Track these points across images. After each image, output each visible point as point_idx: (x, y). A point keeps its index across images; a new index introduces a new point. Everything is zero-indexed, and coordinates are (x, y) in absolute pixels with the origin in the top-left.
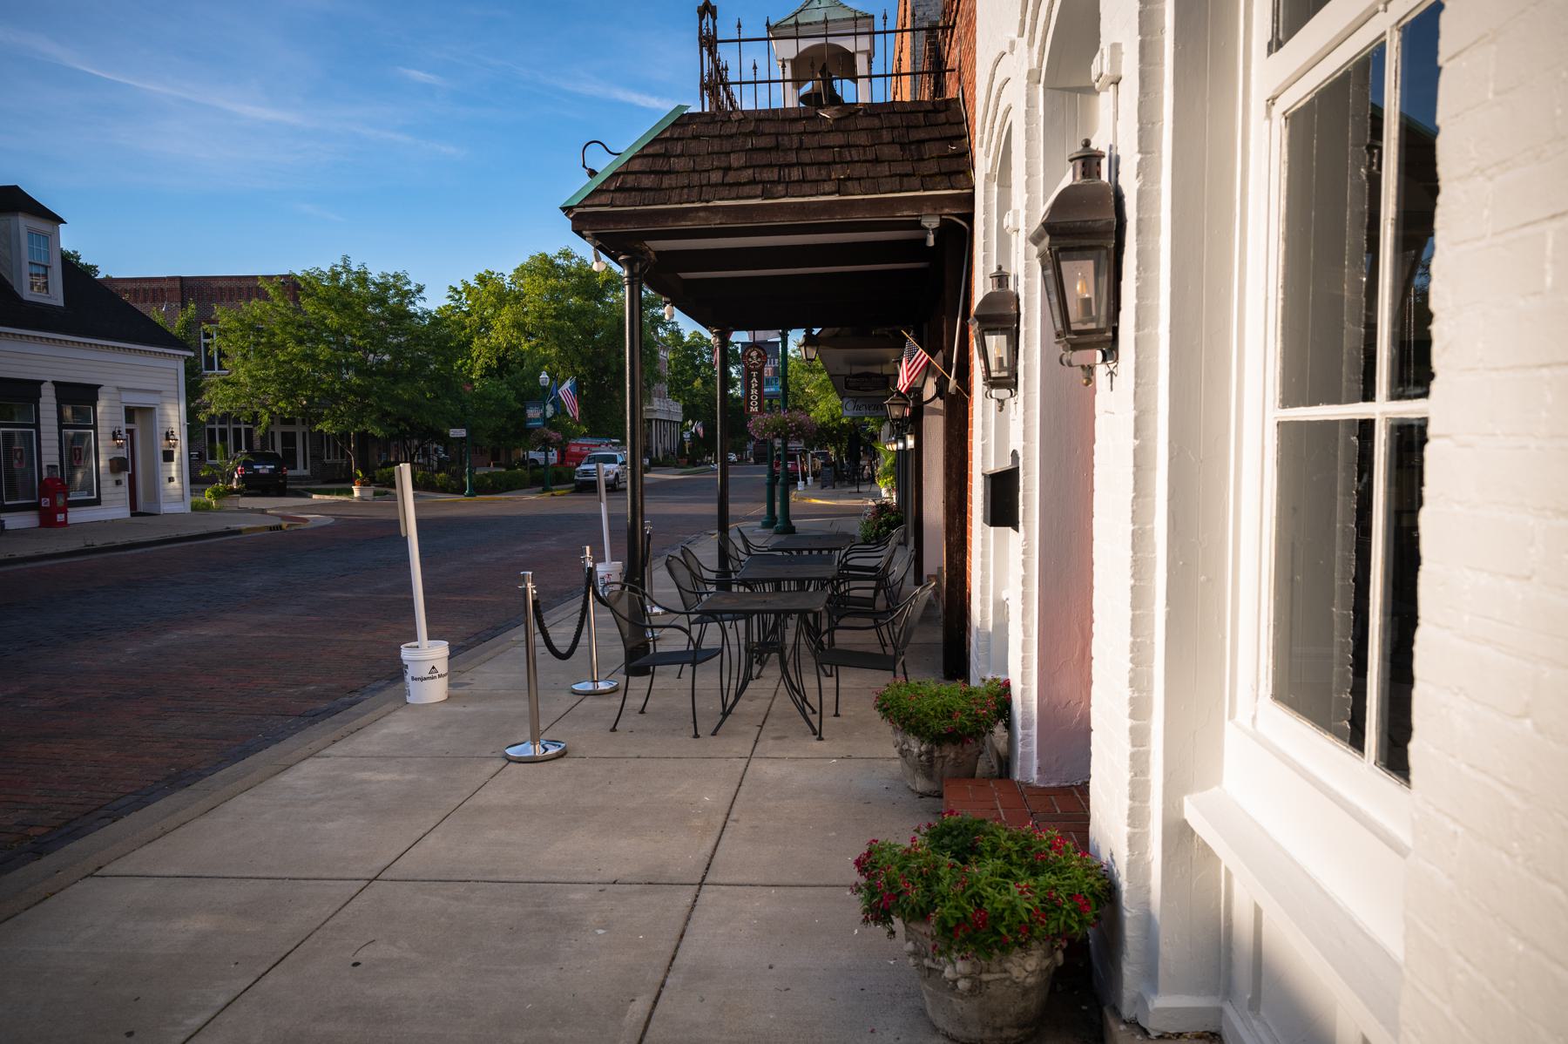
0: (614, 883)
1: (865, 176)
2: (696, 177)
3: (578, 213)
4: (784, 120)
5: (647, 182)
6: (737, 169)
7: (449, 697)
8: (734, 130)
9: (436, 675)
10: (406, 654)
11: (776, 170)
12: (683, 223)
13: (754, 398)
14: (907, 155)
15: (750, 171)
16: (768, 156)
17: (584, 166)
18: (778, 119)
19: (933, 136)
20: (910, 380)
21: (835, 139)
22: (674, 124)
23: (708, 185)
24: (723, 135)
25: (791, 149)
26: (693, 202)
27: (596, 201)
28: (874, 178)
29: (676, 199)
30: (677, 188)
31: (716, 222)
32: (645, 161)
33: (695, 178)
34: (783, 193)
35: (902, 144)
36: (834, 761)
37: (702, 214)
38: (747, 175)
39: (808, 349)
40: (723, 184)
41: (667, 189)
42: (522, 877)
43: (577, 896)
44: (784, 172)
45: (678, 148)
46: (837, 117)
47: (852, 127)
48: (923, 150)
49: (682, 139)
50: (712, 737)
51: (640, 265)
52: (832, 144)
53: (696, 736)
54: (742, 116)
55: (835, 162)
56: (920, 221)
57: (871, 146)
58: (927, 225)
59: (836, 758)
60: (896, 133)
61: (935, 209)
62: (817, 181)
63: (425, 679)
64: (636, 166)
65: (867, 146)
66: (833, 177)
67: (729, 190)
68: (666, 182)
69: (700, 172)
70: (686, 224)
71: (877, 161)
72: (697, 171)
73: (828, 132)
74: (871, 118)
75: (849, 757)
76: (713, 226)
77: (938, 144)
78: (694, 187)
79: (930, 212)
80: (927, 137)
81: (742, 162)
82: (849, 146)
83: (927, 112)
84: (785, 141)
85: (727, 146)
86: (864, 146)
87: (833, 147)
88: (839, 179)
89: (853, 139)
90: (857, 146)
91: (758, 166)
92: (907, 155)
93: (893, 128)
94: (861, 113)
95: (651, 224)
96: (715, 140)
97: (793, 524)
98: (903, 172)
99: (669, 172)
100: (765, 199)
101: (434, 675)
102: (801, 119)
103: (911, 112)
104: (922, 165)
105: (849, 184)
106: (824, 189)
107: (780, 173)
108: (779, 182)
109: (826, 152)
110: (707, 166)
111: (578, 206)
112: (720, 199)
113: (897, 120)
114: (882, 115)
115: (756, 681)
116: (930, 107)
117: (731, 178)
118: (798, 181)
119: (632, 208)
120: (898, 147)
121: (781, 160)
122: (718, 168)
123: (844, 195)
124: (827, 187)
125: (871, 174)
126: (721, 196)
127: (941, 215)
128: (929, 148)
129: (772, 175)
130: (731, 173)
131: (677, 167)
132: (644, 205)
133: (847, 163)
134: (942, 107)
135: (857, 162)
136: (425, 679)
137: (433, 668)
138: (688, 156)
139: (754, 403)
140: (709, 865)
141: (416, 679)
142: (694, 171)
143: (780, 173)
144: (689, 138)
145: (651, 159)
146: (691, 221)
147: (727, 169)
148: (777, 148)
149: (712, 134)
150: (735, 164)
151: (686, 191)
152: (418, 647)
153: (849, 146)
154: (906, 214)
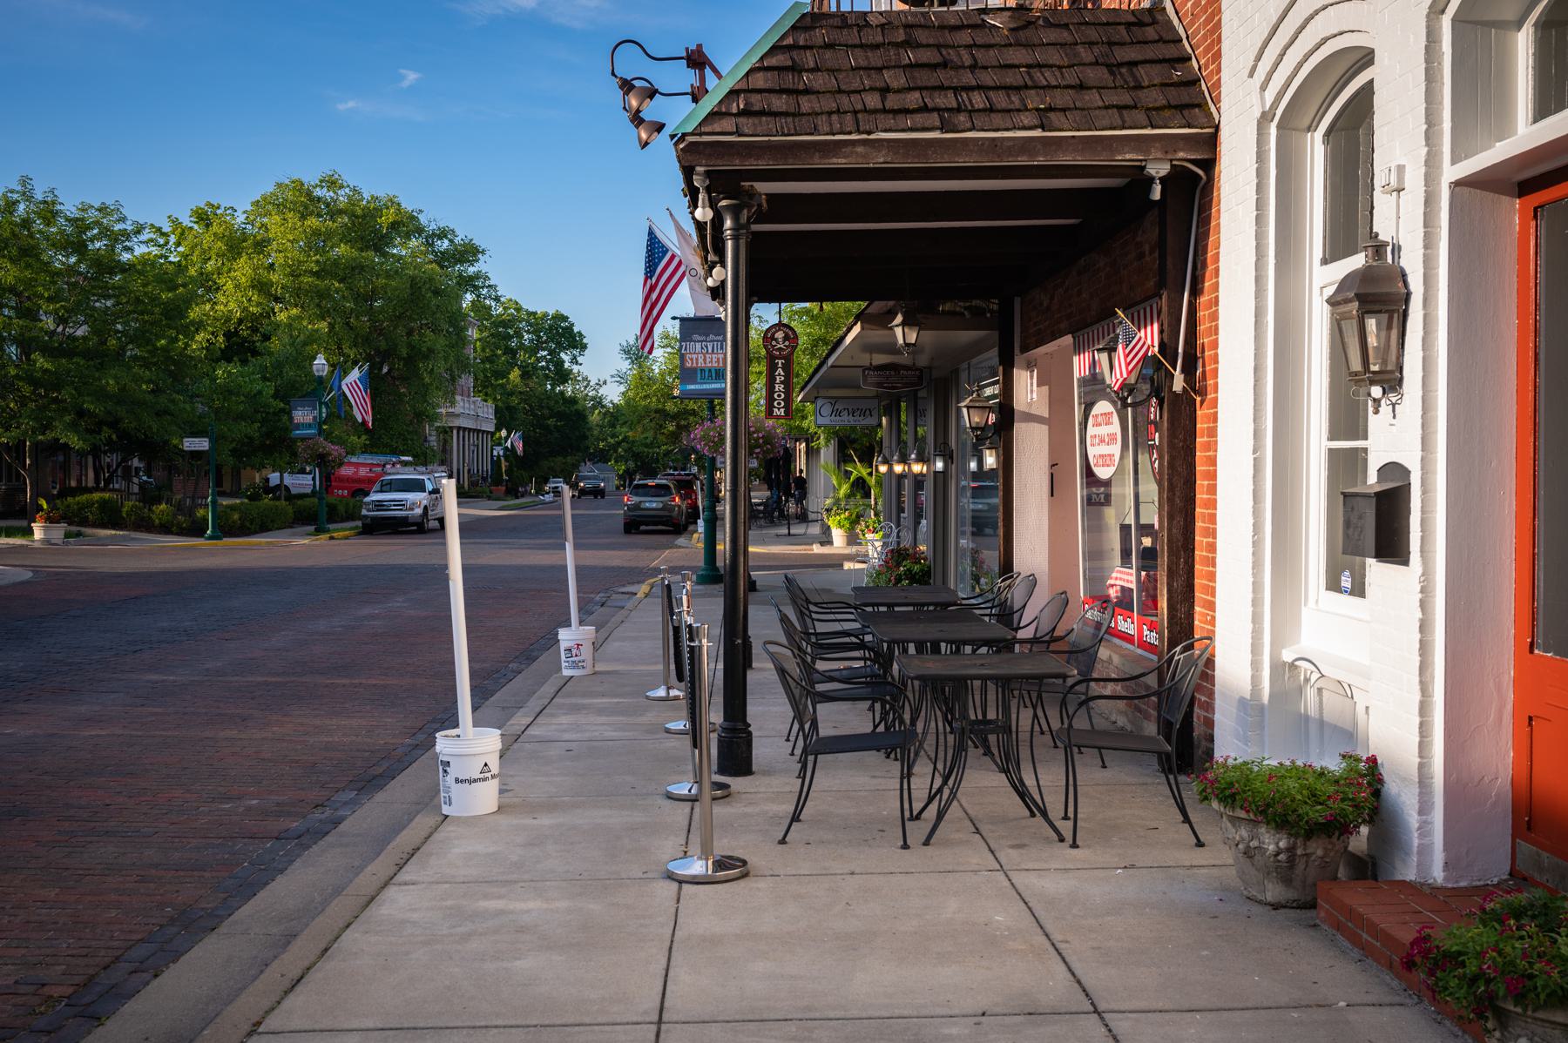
0: (983, 1014)
4: (942, 27)
5: (779, 103)
6: (899, 91)
8: (879, 39)
9: (489, 775)
11: (950, 94)
12: (835, 160)
13: (779, 396)
15: (917, 95)
16: (935, 75)
17: (613, 74)
21: (1017, 56)
22: (794, 28)
23: (865, 111)
24: (867, 46)
25: (963, 67)
26: (850, 133)
29: (827, 129)
30: (822, 113)
31: (879, 160)
32: (769, 74)
33: (845, 102)
34: (969, 125)
36: (1119, 871)
37: (860, 149)
38: (913, 99)
39: (906, 330)
40: (885, 111)
41: (809, 114)
43: (954, 1031)
45: (809, 59)
46: (1012, 26)
47: (1036, 41)
48: (1138, 75)
49: (811, 48)
53: (905, 846)
54: (884, 21)
55: (1026, 87)
56: (1145, 167)
57: (1069, 67)
58: (1153, 172)
60: (1096, 50)
61: (1166, 152)
62: (1009, 111)
63: (475, 781)
64: (760, 81)
65: (1064, 67)
66: (1030, 106)
67: (894, 119)
68: (806, 104)
69: (849, 93)
71: (1081, 87)
72: (844, 92)
73: (1005, 46)
74: (1058, 30)
75: (1133, 866)
76: (871, 165)
77: (1157, 68)
78: (846, 112)
79: (1159, 155)
80: (1140, 58)
81: (902, 81)
82: (1040, 66)
83: (1129, 25)
84: (952, 54)
85: (876, 58)
86: (1060, 67)
87: (1018, 67)
88: (1038, 110)
90: (1051, 66)
91: (926, 88)
93: (1091, 44)
95: (791, 161)
97: (754, 578)
99: (807, 91)
100: (947, 132)
103: (1108, 24)
104: (1141, 94)
105: (1052, 115)
107: (957, 99)
108: (959, 110)
109: (1010, 72)
110: (856, 85)
111: (692, 134)
112: (886, 131)
113: (1093, 34)
114: (1071, 27)
116: (1132, 19)
117: (893, 101)
118: (984, 110)
120: (1105, 70)
121: (955, 80)
122: (872, 89)
123: (1050, 131)
124: (1026, 119)
125: (1078, 104)
126: (888, 127)
127: (1171, 160)
129: (949, 100)
132: (784, 135)
133: (1043, 88)
134: (1147, 19)
135: (1056, 87)
136: (475, 781)
137: (486, 765)
138: (827, 70)
139: (779, 404)
141: (462, 781)
142: (840, 91)
143: (957, 99)
144: (821, 47)
146: (844, 157)
147: (885, 91)
148: (945, 65)
149: (850, 42)
150: (895, 85)
151: (835, 117)
152: (459, 736)
154: (1129, 157)
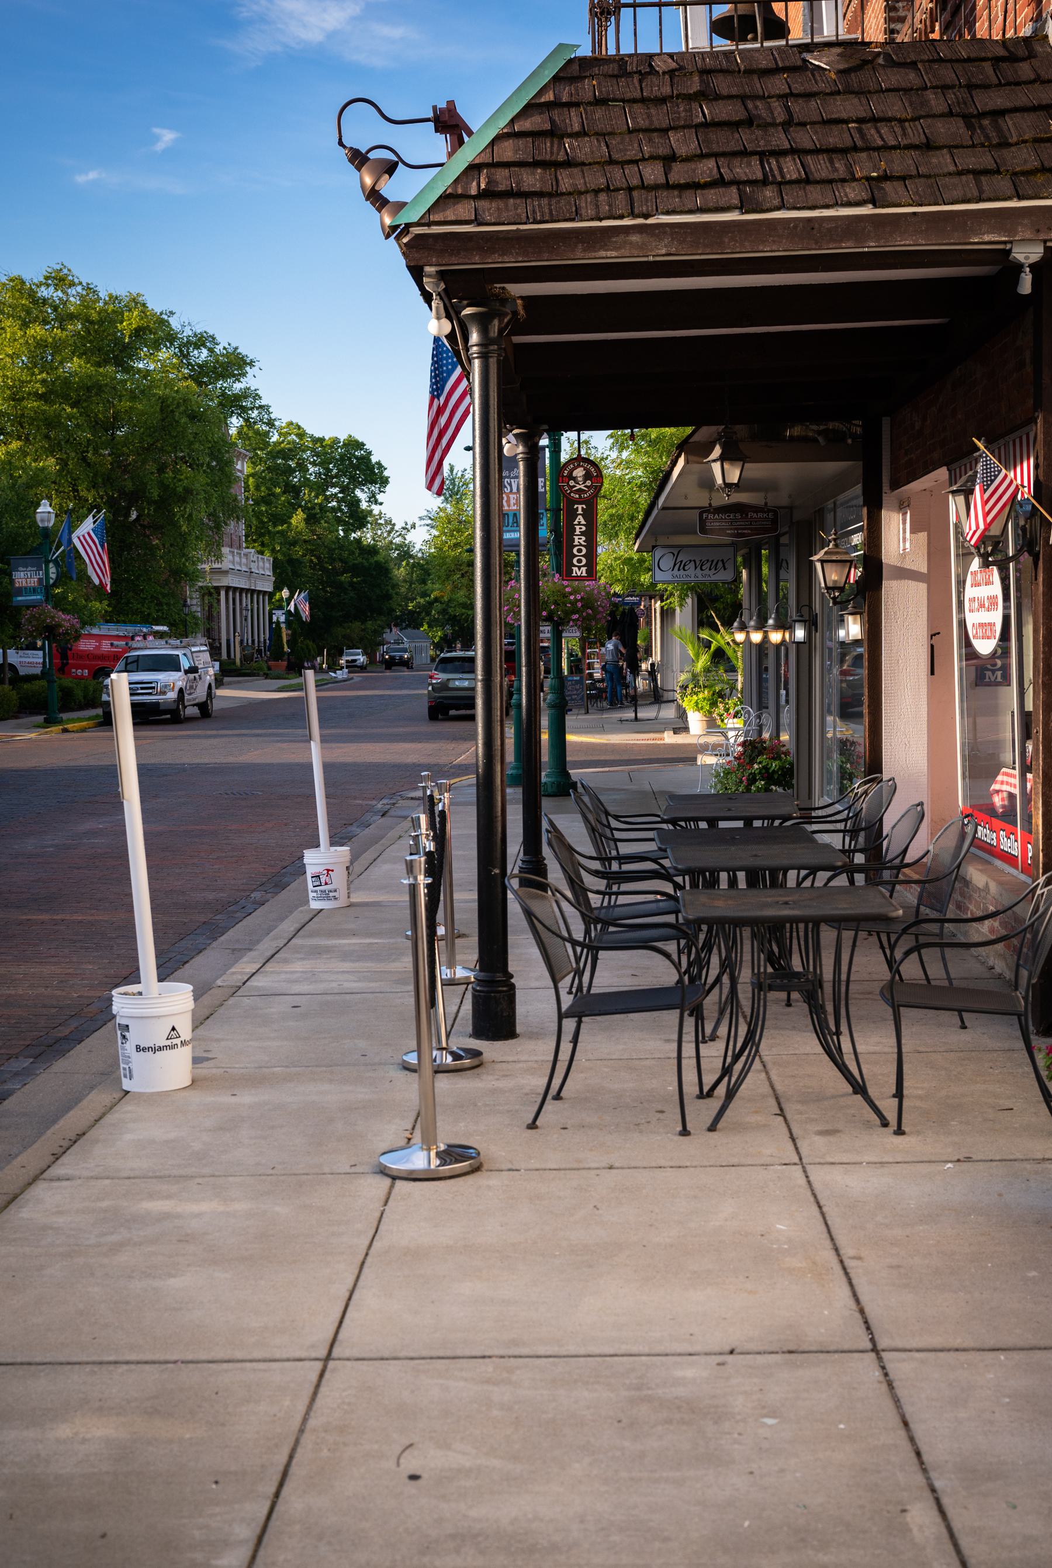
0: (732, 1352)
1: (914, 172)
2: (616, 173)
3: (418, 236)
4: (749, 72)
5: (532, 180)
6: (687, 159)
7: (193, 1081)
8: (666, 90)
9: (177, 1041)
10: (122, 1003)
11: (755, 161)
12: (603, 253)
13: (580, 551)
14: (979, 138)
15: (711, 163)
16: (737, 136)
17: (341, 143)
18: (739, 71)
19: (1018, 104)
20: (989, 519)
21: (847, 107)
22: (556, 79)
23: (643, 187)
24: (649, 100)
25: (774, 125)
26: (621, 217)
27: (450, 215)
28: (929, 177)
29: (591, 212)
30: (587, 192)
31: (660, 252)
32: (521, 142)
33: (617, 175)
34: (776, 202)
35: (966, 117)
36: (949, 1165)
37: (635, 238)
38: (706, 169)
39: (726, 466)
40: (668, 186)
41: (570, 194)
42: (572, 1349)
43: (689, 1373)
44: (769, 164)
45: (574, 120)
46: (841, 67)
47: (872, 86)
48: (1005, 128)
49: (577, 105)
50: (711, 1134)
51: (500, 322)
52: (844, 115)
53: (685, 1132)
54: (674, 65)
55: (855, 149)
56: (1010, 251)
57: (913, 119)
58: (1021, 258)
59: (951, 1162)
60: (951, 96)
61: (1038, 231)
62: (830, 182)
63: (160, 1049)
64: (508, 151)
65: (906, 120)
66: (858, 175)
67: (680, 197)
68: (567, 180)
69: (623, 164)
70: (608, 255)
71: (928, 146)
72: (617, 163)
73: (832, 94)
74: (902, 70)
75: (968, 1159)
76: (651, 259)
77: (1030, 118)
78: (617, 190)
79: (1028, 235)
80: (1009, 105)
81: (693, 146)
82: (874, 120)
83: (997, 60)
84: (760, 108)
85: (660, 117)
86: (901, 121)
87: (846, 122)
88: (869, 179)
89: (876, 106)
90: (889, 120)
91: (724, 154)
92: (979, 138)
93: (945, 88)
94: (881, 61)
95: (546, 256)
96: (636, 106)
97: (574, 778)
98: (977, 167)
99: (568, 164)
100: (747, 212)
101: (175, 1041)
102: (776, 70)
103: (969, 60)
104: (1005, 152)
105: (888, 186)
106: (846, 195)
107: (763, 167)
108: (765, 182)
109: (835, 129)
110: (632, 153)
111: (418, 224)
112: (668, 213)
113: (947, 74)
114: (920, 66)
115: (711, 1043)
116: (1001, 52)
117: (679, 173)
118: (797, 182)
119: (514, 227)
120: (961, 123)
121: (762, 143)
122: (653, 158)
123: (883, 207)
124: (852, 191)
125: (923, 170)
126: (671, 208)
127: (1045, 241)
128: (1014, 124)
129: (749, 169)
130: (676, 167)
131: (581, 156)
132: (535, 222)
133: (878, 149)
134: (1022, 52)
135: (894, 148)
136: (160, 1049)
137: (173, 1029)
138: (597, 134)
139: (579, 561)
140: (866, 1322)
141: (144, 1049)
142: (611, 162)
143: (763, 167)
144: (590, 104)
145: (530, 140)
146: (615, 249)
147: (669, 159)
148: (749, 122)
149: (628, 96)
150: (682, 151)
151: (603, 197)
152: (140, 994)
153: (874, 120)
154: (988, 238)
